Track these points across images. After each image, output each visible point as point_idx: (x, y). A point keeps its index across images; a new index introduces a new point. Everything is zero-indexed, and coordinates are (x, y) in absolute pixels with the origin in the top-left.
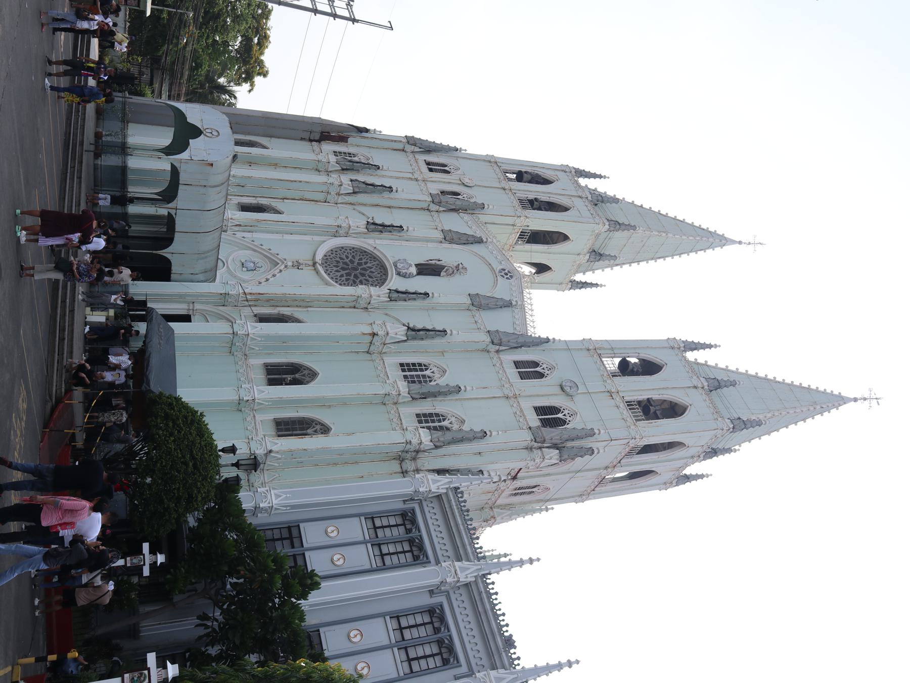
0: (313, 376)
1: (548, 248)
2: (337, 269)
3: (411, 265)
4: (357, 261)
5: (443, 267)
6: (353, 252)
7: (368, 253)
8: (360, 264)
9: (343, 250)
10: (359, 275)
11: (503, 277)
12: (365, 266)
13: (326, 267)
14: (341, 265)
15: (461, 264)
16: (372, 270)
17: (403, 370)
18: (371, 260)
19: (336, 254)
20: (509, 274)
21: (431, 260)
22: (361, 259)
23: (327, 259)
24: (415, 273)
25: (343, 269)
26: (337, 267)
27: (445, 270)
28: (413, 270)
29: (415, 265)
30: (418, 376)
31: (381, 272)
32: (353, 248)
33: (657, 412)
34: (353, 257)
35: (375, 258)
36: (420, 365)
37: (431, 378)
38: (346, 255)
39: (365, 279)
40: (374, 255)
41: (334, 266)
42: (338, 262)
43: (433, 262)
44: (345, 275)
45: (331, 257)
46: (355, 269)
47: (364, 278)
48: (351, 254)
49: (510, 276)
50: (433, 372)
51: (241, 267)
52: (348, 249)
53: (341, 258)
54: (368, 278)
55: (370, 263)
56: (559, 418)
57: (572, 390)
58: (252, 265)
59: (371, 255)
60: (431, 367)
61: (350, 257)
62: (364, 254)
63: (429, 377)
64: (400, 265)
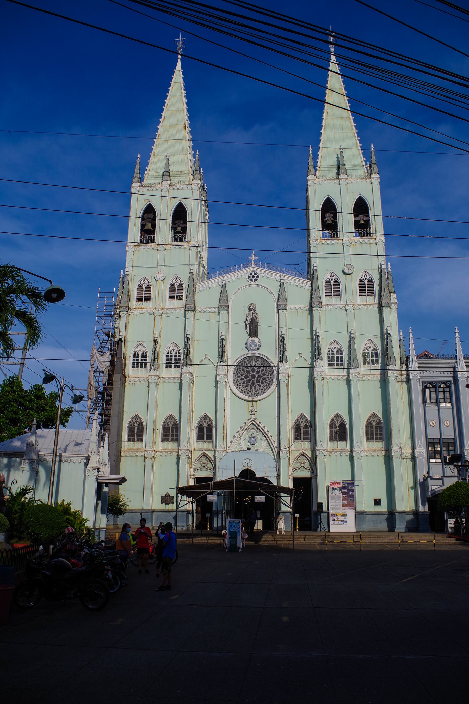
2: (253, 387)
3: (253, 341)
4: (246, 373)
6: (238, 374)
9: (236, 380)
14: (250, 384)
19: (240, 385)
20: (253, 274)
25: (253, 383)
26: (251, 387)
28: (256, 340)
30: (337, 357)
31: (254, 360)
34: (242, 375)
35: (242, 361)
37: (338, 350)
42: (247, 386)
43: (248, 326)
46: (253, 376)
47: (260, 372)
52: (235, 377)
53: (244, 383)
56: (367, 283)
58: (253, 439)
60: (331, 348)
61: (243, 377)
64: (253, 347)
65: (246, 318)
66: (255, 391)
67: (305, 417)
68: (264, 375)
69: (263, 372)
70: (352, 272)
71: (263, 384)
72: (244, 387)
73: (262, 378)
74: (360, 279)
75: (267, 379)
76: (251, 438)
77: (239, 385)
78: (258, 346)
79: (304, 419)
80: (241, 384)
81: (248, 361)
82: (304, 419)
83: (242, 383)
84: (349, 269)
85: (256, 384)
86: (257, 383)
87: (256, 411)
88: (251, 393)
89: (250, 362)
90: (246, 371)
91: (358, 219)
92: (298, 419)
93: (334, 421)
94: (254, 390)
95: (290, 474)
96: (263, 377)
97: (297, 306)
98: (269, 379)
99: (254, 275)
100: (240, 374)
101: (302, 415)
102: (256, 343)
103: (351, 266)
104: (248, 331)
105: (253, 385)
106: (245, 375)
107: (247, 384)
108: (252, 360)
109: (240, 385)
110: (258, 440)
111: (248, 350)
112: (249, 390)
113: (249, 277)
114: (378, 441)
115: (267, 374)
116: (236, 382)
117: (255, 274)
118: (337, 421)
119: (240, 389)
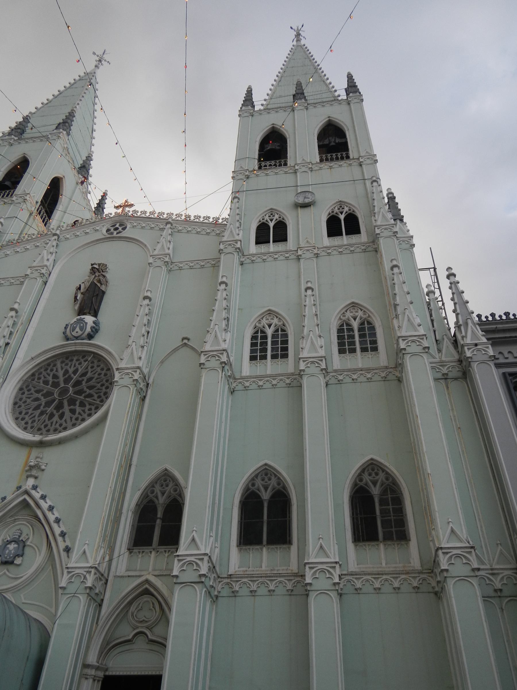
0: (266, 474)
1: (62, 205)
5: (93, 283)
7: (36, 371)
8: (56, 385)
10: (78, 388)
11: (120, 232)
12: (61, 379)
13: (48, 431)
15: (92, 265)
16: (71, 370)
17: (264, 357)
18: (52, 370)
20: (117, 226)
21: (76, 297)
22: (46, 383)
23: (32, 427)
24: (94, 319)
25: (60, 406)
26: (52, 416)
27: (99, 285)
28: (89, 319)
29: (79, 315)
30: (273, 343)
31: (77, 360)
32: (21, 389)
33: (337, 142)
34: (38, 392)
35: (49, 365)
36: (254, 338)
38: (32, 401)
39: (86, 382)
40: (43, 364)
41: (49, 419)
42: (42, 413)
43: (79, 296)
44: (72, 407)
45: (30, 422)
47: (84, 383)
48: (32, 394)
49: (119, 226)
50: (270, 326)
51: (11, 567)
52: (20, 396)
53: (37, 408)
54: (85, 379)
55: (57, 371)
57: (311, 197)
59: (41, 368)
60: (260, 326)
61: (39, 395)
62: (37, 376)
63: (277, 331)
65: (80, 285)
66: (58, 425)
67: (174, 479)
68: (91, 388)
69: (91, 383)
70: (311, 201)
71: (83, 408)
72: (34, 417)
73: (83, 395)
74: (329, 214)
75: (96, 396)
76: (9, 542)
77: (23, 413)
78: (88, 330)
79: (171, 485)
80: (30, 411)
81: (62, 362)
82: (170, 486)
83: (33, 407)
84: (305, 198)
85: (66, 408)
86: (69, 405)
87: (43, 467)
88: (47, 429)
89: (67, 364)
90: (50, 383)
91: (326, 142)
92: (153, 486)
93: (256, 486)
94: (57, 422)
95: (92, 659)
96: (87, 393)
97: (192, 261)
98: (99, 397)
99: (119, 227)
100: (35, 389)
101: (165, 475)
102: (86, 323)
103: (310, 194)
104: (77, 307)
105: (58, 412)
106: (45, 392)
107: (45, 409)
108: (72, 360)
109: (26, 413)
110: (28, 551)
111: (68, 339)
112: (45, 421)
113: (108, 230)
114: (389, 543)
115: (99, 385)
116: (20, 406)
117: (120, 225)
118: (266, 488)
119: (23, 422)
